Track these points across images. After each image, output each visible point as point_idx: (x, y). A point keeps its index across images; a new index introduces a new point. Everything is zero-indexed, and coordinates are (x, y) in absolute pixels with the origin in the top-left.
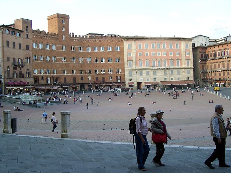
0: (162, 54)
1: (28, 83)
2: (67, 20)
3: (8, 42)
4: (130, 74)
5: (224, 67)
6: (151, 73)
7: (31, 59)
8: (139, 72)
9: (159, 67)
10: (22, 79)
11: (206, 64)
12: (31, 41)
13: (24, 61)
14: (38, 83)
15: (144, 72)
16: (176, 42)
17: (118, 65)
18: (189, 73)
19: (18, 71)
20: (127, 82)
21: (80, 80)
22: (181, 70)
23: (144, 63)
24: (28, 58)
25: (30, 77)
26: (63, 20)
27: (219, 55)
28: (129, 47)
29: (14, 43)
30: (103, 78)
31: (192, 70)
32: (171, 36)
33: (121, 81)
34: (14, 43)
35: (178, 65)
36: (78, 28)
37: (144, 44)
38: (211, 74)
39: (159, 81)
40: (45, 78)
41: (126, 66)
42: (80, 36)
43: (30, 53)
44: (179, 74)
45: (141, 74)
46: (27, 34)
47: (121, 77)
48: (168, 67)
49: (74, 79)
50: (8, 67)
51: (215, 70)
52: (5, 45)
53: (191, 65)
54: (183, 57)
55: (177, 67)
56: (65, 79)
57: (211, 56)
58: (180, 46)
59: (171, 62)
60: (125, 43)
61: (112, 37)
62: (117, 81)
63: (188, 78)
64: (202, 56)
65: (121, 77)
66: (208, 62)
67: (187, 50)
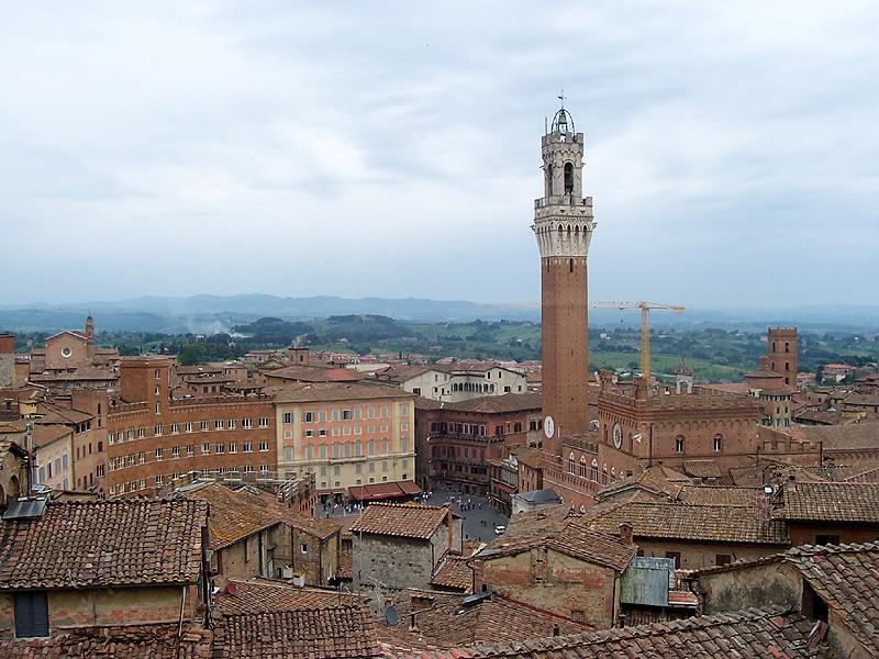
5: (475, 456)
6: (331, 471)
16: (382, 404)
18: (405, 466)
22: (390, 462)
27: (466, 431)
41: (280, 458)
44: (385, 470)
51: (458, 459)
55: (383, 456)
57: (451, 429)
59: (371, 446)
63: (405, 476)
67: (405, 419)
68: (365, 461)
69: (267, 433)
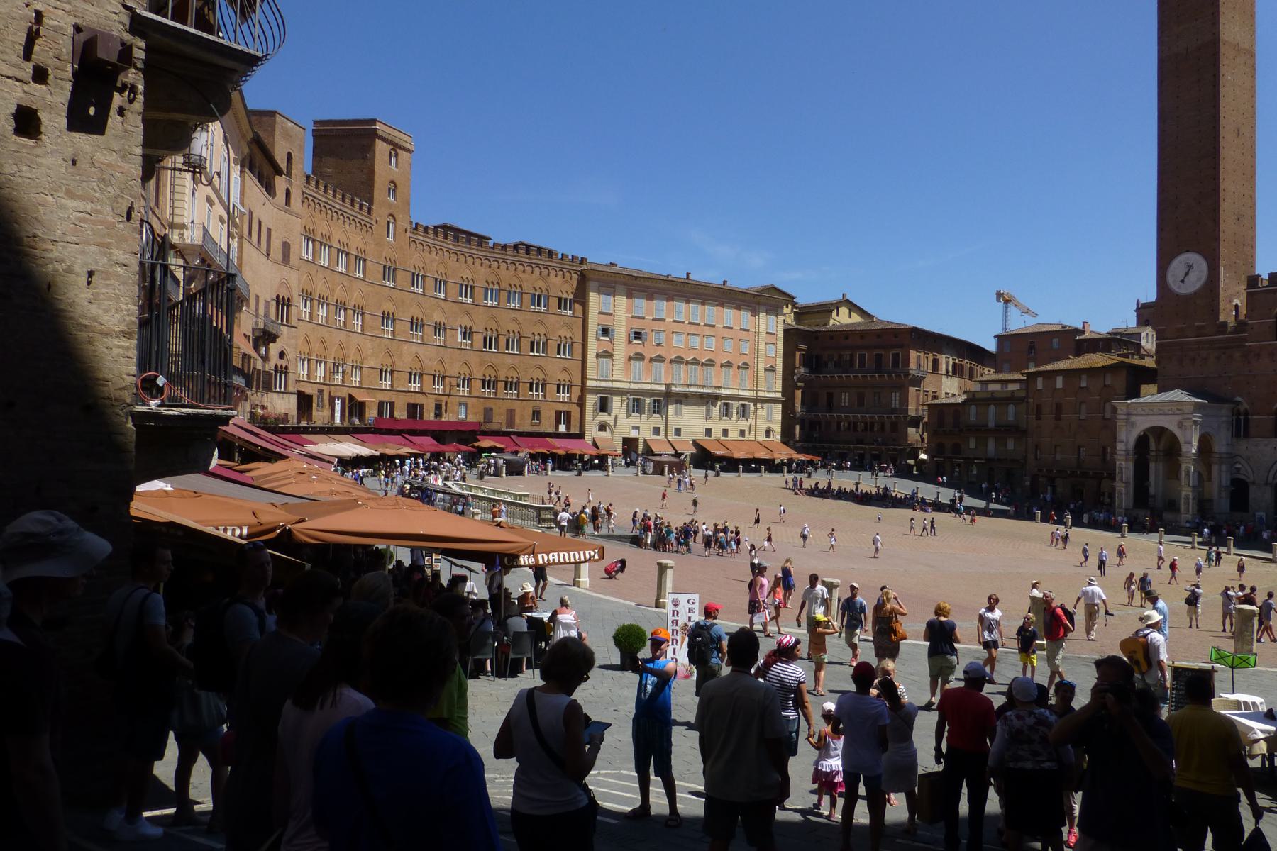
4: (604, 406)
7: (293, 309)
12: (297, 225)
14: (310, 418)
17: (565, 369)
18: (769, 417)
30: (511, 414)
31: (780, 406)
33: (568, 428)
41: (591, 373)
46: (288, 193)
62: (557, 428)
63: (768, 433)
68: (717, 397)
69: (569, 326)
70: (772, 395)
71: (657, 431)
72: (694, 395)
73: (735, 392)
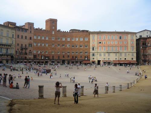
0: (114, 43)
1: (30, 58)
2: (56, 22)
3: (18, 36)
4: (93, 55)
6: (107, 55)
7: (32, 45)
8: (99, 54)
9: (112, 51)
10: (26, 56)
11: (146, 49)
12: (33, 35)
13: (27, 46)
15: (102, 54)
19: (24, 51)
20: (91, 60)
21: (62, 58)
22: (127, 54)
23: (102, 48)
24: (30, 45)
25: (31, 55)
26: (52, 22)
28: (93, 38)
29: (22, 36)
31: (136, 53)
32: (123, 31)
34: (22, 36)
35: (125, 50)
36: (63, 26)
37: (104, 37)
38: (149, 56)
39: (112, 60)
40: (40, 56)
42: (63, 31)
43: (32, 41)
44: (125, 56)
45: (100, 55)
46: (31, 31)
47: (87, 57)
48: (118, 51)
49: (59, 57)
50: (18, 49)
52: (17, 37)
53: (135, 50)
54: (129, 45)
56: (53, 57)
58: (127, 38)
59: (121, 48)
60: (91, 35)
61: (83, 31)
64: (143, 44)
65: (87, 57)
66: (147, 48)
67: (132, 40)
70: (133, 51)
71: (104, 59)
72: (111, 52)
73: (123, 51)
